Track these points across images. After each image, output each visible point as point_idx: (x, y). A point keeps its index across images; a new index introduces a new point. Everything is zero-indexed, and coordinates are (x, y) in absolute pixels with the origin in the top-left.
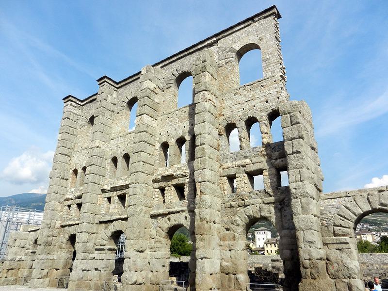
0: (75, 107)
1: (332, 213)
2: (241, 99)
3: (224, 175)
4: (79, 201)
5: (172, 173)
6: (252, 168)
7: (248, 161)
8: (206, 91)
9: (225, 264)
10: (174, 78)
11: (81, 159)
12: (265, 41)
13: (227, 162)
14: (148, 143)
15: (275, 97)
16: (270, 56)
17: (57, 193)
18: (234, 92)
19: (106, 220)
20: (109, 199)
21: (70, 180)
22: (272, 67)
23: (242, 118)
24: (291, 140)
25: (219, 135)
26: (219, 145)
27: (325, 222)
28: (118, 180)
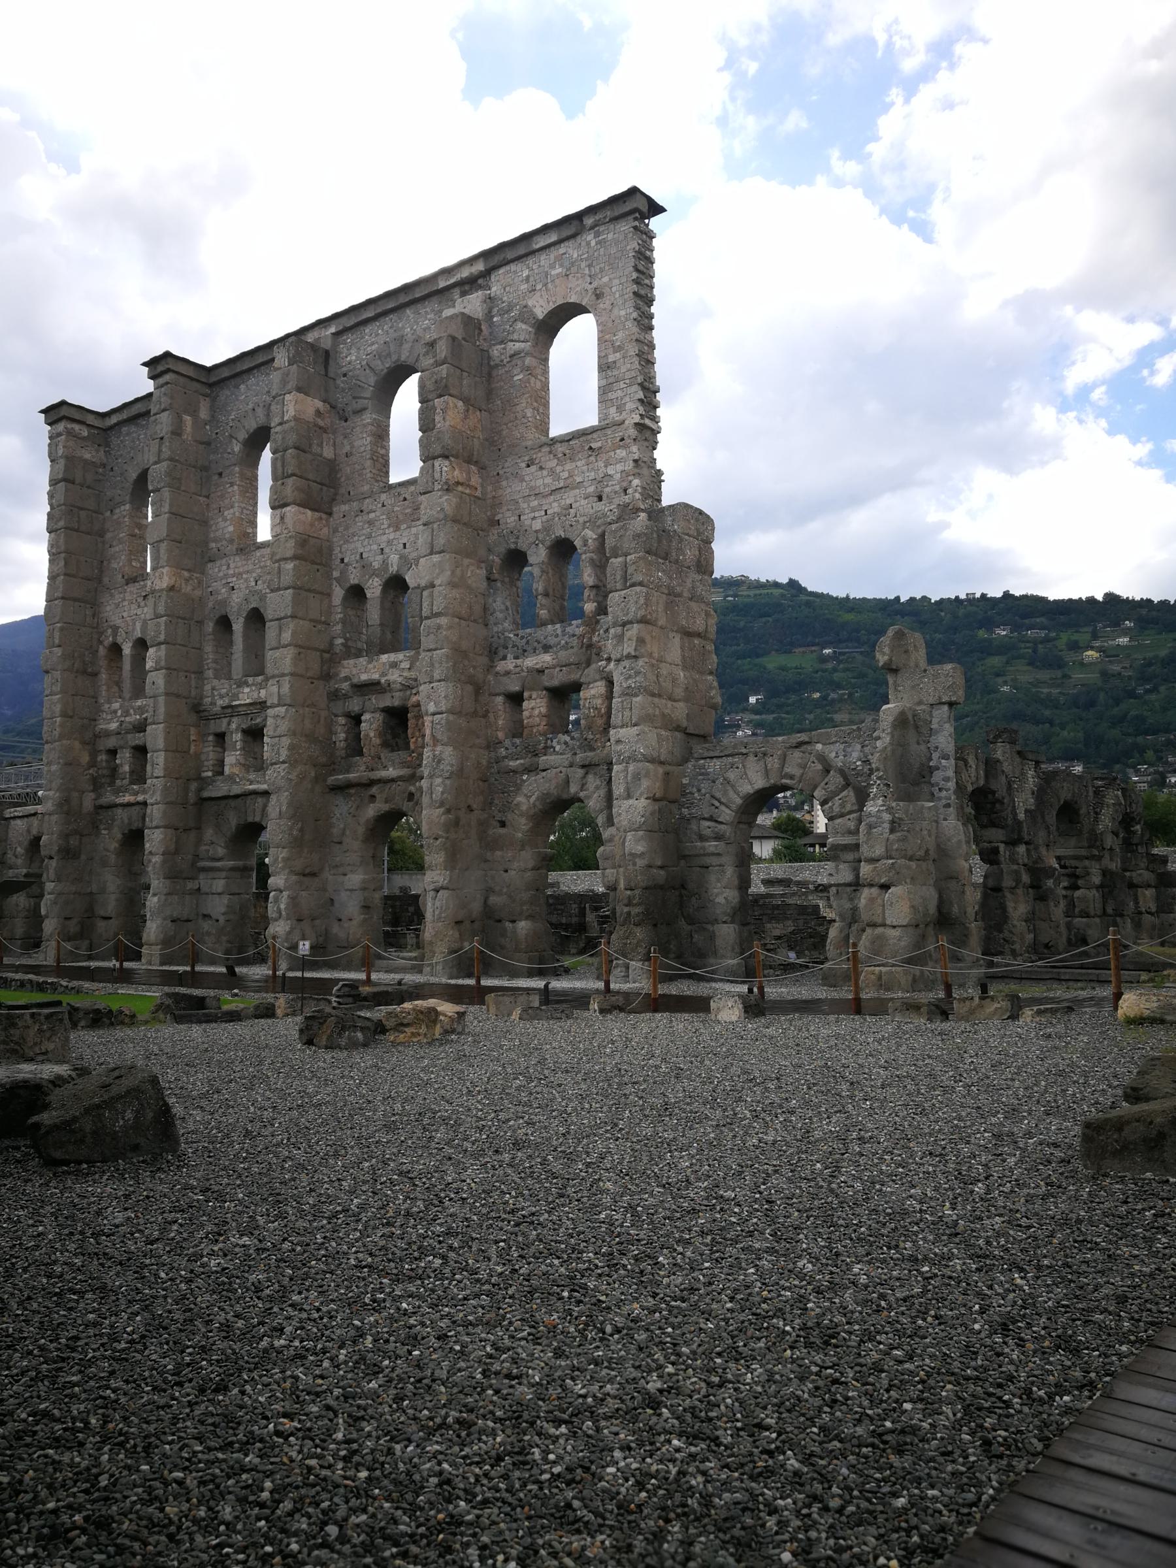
0: (84, 438)
1: (703, 791)
2: (543, 481)
3: (497, 691)
4: (136, 739)
5: (376, 676)
6: (558, 678)
7: (547, 658)
8: (446, 457)
9: (493, 899)
10: (372, 380)
11: (125, 614)
12: (607, 305)
13: (504, 658)
14: (309, 590)
15: (617, 488)
16: (618, 355)
17: (71, 717)
18: (526, 458)
19: (220, 795)
20: (221, 737)
21: (104, 676)
22: (620, 393)
23: (541, 536)
24: (624, 625)
25: (488, 579)
26: (485, 609)
27: (685, 811)
28: (238, 686)
